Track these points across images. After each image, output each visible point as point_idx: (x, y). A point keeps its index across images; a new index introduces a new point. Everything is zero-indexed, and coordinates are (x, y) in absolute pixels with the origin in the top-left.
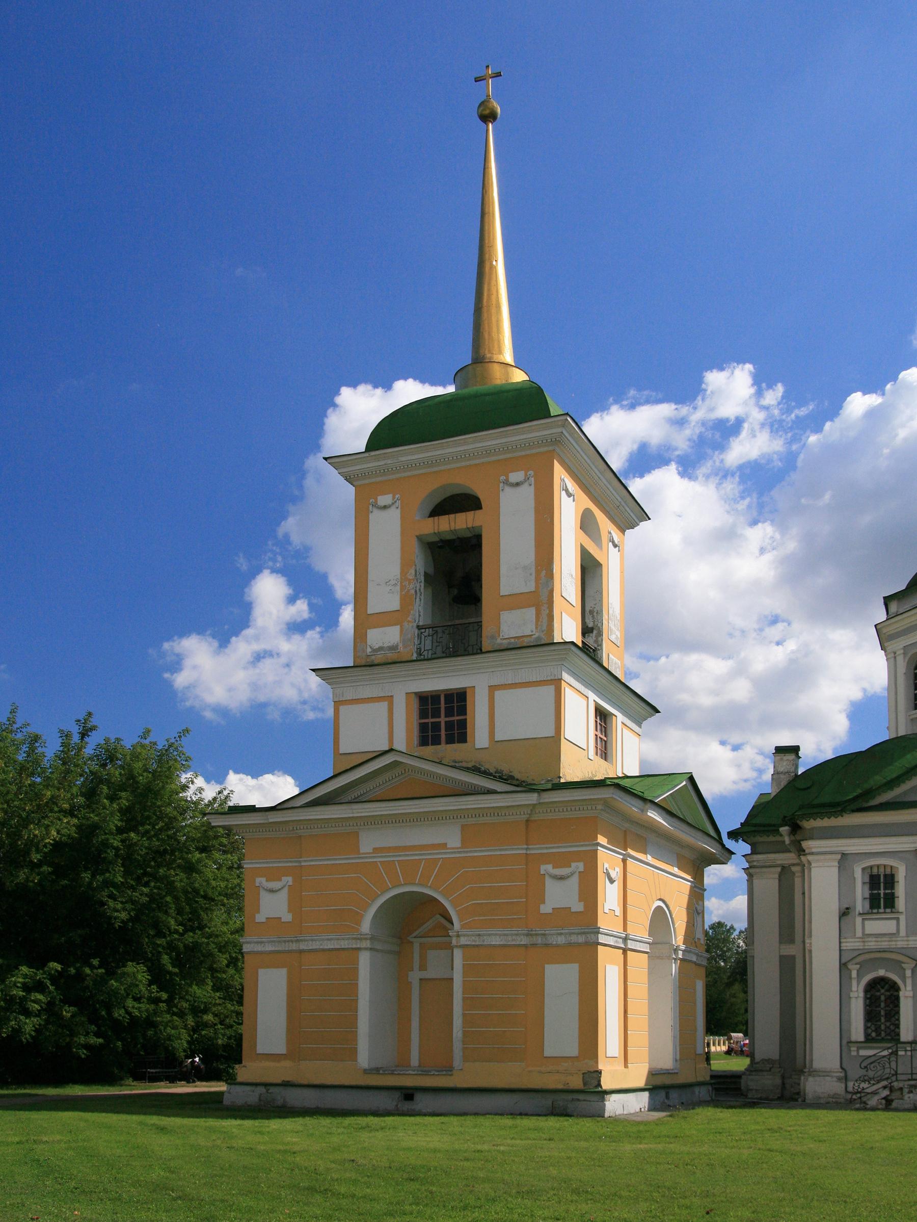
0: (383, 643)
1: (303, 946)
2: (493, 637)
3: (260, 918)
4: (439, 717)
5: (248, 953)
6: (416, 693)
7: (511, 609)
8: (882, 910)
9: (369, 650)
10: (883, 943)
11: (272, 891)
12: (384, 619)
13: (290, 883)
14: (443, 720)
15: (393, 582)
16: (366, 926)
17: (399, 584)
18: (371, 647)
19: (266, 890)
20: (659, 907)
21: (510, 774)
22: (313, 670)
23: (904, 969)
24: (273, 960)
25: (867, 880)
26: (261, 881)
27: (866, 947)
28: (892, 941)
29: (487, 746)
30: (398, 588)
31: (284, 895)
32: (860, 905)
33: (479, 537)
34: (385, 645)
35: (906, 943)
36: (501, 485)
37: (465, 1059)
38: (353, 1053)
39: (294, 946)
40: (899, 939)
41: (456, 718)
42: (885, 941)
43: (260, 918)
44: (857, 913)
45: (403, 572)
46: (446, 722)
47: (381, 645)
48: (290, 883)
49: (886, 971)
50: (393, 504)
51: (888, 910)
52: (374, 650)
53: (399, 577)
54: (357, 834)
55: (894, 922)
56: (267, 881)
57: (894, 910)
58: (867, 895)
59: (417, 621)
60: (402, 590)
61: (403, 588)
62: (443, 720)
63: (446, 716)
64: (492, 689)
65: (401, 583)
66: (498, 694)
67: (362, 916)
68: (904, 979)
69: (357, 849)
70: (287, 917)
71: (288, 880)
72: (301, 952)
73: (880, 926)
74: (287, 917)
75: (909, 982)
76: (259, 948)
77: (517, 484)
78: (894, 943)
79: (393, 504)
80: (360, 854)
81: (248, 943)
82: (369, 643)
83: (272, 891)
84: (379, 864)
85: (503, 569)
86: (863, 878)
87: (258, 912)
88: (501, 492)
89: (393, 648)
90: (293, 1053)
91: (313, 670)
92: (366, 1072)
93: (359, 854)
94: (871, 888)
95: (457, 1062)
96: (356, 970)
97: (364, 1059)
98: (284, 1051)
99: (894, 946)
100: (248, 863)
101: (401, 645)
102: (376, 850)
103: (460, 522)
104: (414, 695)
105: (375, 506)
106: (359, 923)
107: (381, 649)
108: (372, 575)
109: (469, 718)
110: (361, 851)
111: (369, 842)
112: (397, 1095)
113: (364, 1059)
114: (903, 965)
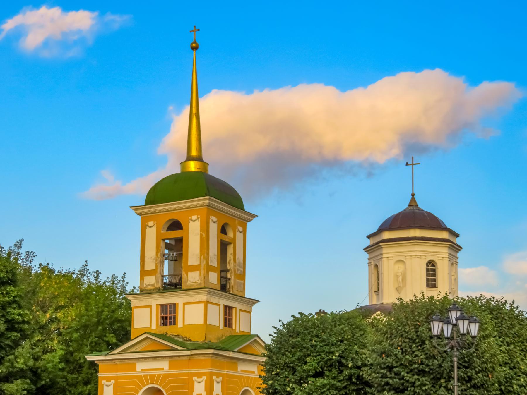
0: (150, 283)
6: (160, 305)
11: (108, 386)
12: (150, 273)
13: (114, 383)
15: (153, 258)
18: (146, 284)
26: (104, 382)
30: (155, 260)
31: (112, 387)
34: (150, 284)
45: (157, 254)
47: (149, 283)
52: (147, 286)
53: (155, 256)
56: (106, 382)
63: (170, 314)
71: (113, 382)
77: (194, 221)
82: (145, 282)
83: (108, 386)
89: (153, 285)
103: (176, 234)
107: (149, 285)
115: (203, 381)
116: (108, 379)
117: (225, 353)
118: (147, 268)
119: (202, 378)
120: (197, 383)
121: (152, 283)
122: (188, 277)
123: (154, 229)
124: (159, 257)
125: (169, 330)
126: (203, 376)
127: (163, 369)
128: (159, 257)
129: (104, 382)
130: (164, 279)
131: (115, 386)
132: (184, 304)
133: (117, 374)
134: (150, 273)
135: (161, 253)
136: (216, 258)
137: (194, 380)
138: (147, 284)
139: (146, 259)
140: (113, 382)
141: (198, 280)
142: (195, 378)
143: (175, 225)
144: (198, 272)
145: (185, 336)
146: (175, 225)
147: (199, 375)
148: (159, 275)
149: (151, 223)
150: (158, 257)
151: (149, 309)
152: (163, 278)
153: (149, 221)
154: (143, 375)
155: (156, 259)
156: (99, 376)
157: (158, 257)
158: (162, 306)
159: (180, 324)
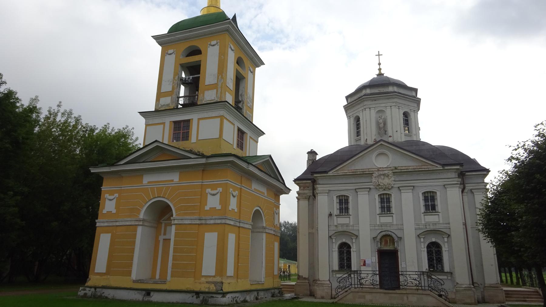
1: (118, 224)
2: (202, 100)
3: (105, 211)
4: (181, 131)
5: (98, 226)
7: (208, 90)
8: (344, 214)
9: (160, 106)
10: (344, 228)
12: (166, 94)
14: (182, 132)
15: (170, 81)
16: (141, 216)
17: (172, 81)
19: (108, 199)
20: (257, 210)
21: (203, 153)
22: (139, 112)
23: (352, 239)
24: (107, 230)
25: (338, 201)
26: (107, 196)
27: (338, 229)
28: (348, 227)
29: (195, 142)
30: (172, 83)
32: (336, 212)
33: (200, 66)
34: (166, 104)
35: (352, 228)
36: (209, 45)
37: (172, 276)
38: (129, 273)
39: (115, 224)
40: (350, 226)
41: (186, 131)
42: (345, 227)
43: (105, 211)
44: (335, 215)
45: (174, 78)
46: (181, 131)
47: (164, 104)
48: (117, 197)
49: (346, 239)
50: (173, 53)
51: (346, 214)
52: (162, 106)
53: (172, 78)
54: (143, 175)
55: (348, 219)
57: (348, 214)
58: (338, 208)
59: (177, 95)
60: (173, 84)
61: (173, 83)
62: (182, 132)
64: (199, 119)
65: (173, 81)
66: (201, 121)
67: (141, 211)
68: (353, 243)
69: (142, 183)
70: (114, 211)
71: (117, 195)
72: (117, 226)
73: (343, 220)
74: (114, 211)
75: (354, 244)
76: (102, 224)
78: (348, 228)
79: (173, 53)
80: (142, 184)
81: (99, 222)
82: (160, 103)
83: (110, 200)
84: (149, 189)
85: (207, 76)
86: (336, 201)
87: (104, 209)
88: (208, 48)
89: (168, 105)
90: (108, 273)
91: (139, 112)
92: (134, 282)
93: (142, 184)
94: (340, 205)
95: (169, 278)
96: (135, 236)
97: (134, 276)
98: (105, 272)
99: (348, 229)
100: (103, 188)
101: (171, 104)
102: (149, 182)
104: (172, 122)
105: (167, 53)
106: (139, 214)
107: (164, 105)
108: (163, 79)
109: (190, 131)
110: (143, 183)
111: (147, 179)
112: (144, 292)
113: (134, 276)
114: (352, 237)
115: (218, 193)
116: (111, 193)
117: (243, 164)
118: (163, 90)
119: (217, 190)
120: (210, 195)
121: (167, 104)
122: (204, 96)
123: (173, 56)
124: (176, 80)
125: (182, 144)
126: (218, 188)
127: (172, 181)
128: (176, 80)
129: (107, 196)
130: (180, 100)
131: (118, 199)
132: (199, 119)
133: (121, 187)
134: (166, 94)
135: (178, 77)
136: (232, 83)
137: (207, 192)
138: (162, 104)
139: (163, 83)
140: (117, 195)
141: (215, 98)
142: (209, 190)
143: (196, 52)
144: (215, 90)
145: (197, 150)
146: (196, 52)
147: (214, 187)
148: (174, 96)
149: (170, 51)
150: (175, 80)
151: (162, 126)
152: (179, 100)
153: (169, 50)
154: (150, 188)
155: (173, 82)
156: (102, 189)
157: (175, 80)
158: (175, 122)
159: (193, 139)
